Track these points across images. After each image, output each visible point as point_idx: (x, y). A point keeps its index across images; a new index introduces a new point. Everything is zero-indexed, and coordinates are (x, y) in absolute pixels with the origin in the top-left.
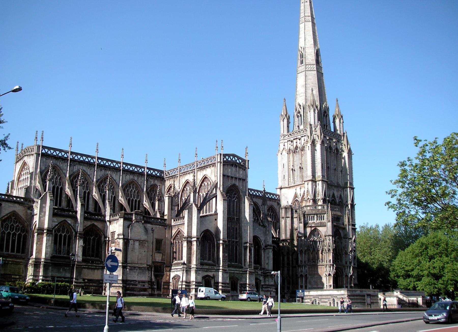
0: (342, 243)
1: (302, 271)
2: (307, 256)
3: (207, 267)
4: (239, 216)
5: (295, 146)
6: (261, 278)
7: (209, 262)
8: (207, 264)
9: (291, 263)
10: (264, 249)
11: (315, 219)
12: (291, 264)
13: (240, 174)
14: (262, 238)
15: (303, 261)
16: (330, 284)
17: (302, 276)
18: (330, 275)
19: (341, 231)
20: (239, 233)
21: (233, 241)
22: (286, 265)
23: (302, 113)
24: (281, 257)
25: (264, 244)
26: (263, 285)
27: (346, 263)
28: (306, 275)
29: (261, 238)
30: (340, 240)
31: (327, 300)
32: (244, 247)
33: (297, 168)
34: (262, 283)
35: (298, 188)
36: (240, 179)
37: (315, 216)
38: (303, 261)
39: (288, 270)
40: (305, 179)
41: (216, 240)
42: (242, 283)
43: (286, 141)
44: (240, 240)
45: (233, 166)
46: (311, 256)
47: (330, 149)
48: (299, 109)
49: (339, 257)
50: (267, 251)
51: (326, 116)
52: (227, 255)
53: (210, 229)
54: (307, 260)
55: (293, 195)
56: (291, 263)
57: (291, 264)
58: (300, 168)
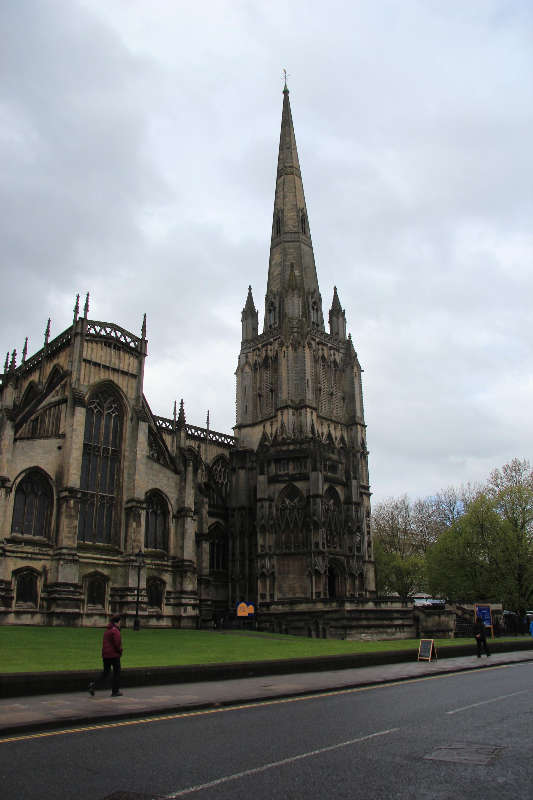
0: (340, 512)
1: (263, 566)
3: (30, 549)
4: (120, 446)
5: (264, 355)
6: (167, 577)
7: (37, 538)
8: (28, 543)
9: (247, 552)
10: (174, 517)
11: (291, 467)
12: (247, 555)
13: (128, 363)
14: (172, 495)
15: (267, 546)
16: (317, 590)
17: (263, 575)
18: (317, 572)
20: (118, 480)
21: (103, 497)
22: (238, 556)
23: (277, 306)
24: (230, 543)
25: (176, 508)
26: (169, 593)
27: (351, 549)
28: (273, 573)
29: (169, 495)
30: (338, 507)
31: (302, 624)
32: (126, 509)
33: (265, 392)
34: (168, 588)
35: (268, 425)
36: (125, 373)
37: (291, 462)
39: (242, 565)
40: (279, 406)
41: (59, 492)
42: (116, 586)
43: (251, 350)
44: (118, 495)
45: (110, 346)
47: (323, 362)
48: (273, 300)
49: (336, 539)
50: (180, 521)
51: (317, 309)
52: (76, 523)
53: (42, 466)
54: (272, 544)
55: (260, 435)
56: (247, 552)
57: (247, 555)
58: (272, 391)
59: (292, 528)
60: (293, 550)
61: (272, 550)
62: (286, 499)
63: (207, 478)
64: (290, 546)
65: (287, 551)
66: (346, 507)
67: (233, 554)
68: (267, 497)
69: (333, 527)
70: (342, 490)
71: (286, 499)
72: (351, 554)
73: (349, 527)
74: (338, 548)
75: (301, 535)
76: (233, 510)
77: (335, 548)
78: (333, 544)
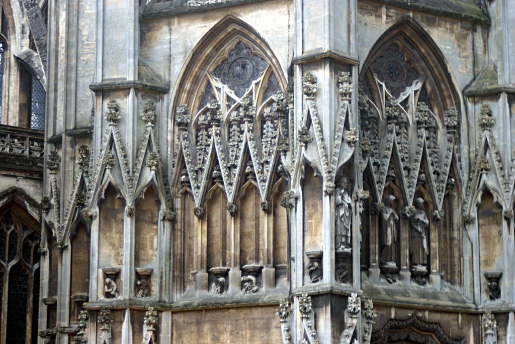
2: (159, 238)
19: (442, 37)
38: (126, 277)
46: (199, 239)
54: (156, 260)
59: (230, 199)
60: (234, 292)
61: (155, 288)
62: (216, 83)
63: (27, 41)
64: (225, 274)
65: (214, 292)
66: (474, 109)
67: (52, 308)
68: (131, 77)
69: (410, 192)
70: (461, 39)
71: (216, 83)
72: (497, 302)
73: (487, 193)
74: (436, 278)
75: (266, 223)
76: (57, 141)
77: (421, 278)
78: (412, 263)
